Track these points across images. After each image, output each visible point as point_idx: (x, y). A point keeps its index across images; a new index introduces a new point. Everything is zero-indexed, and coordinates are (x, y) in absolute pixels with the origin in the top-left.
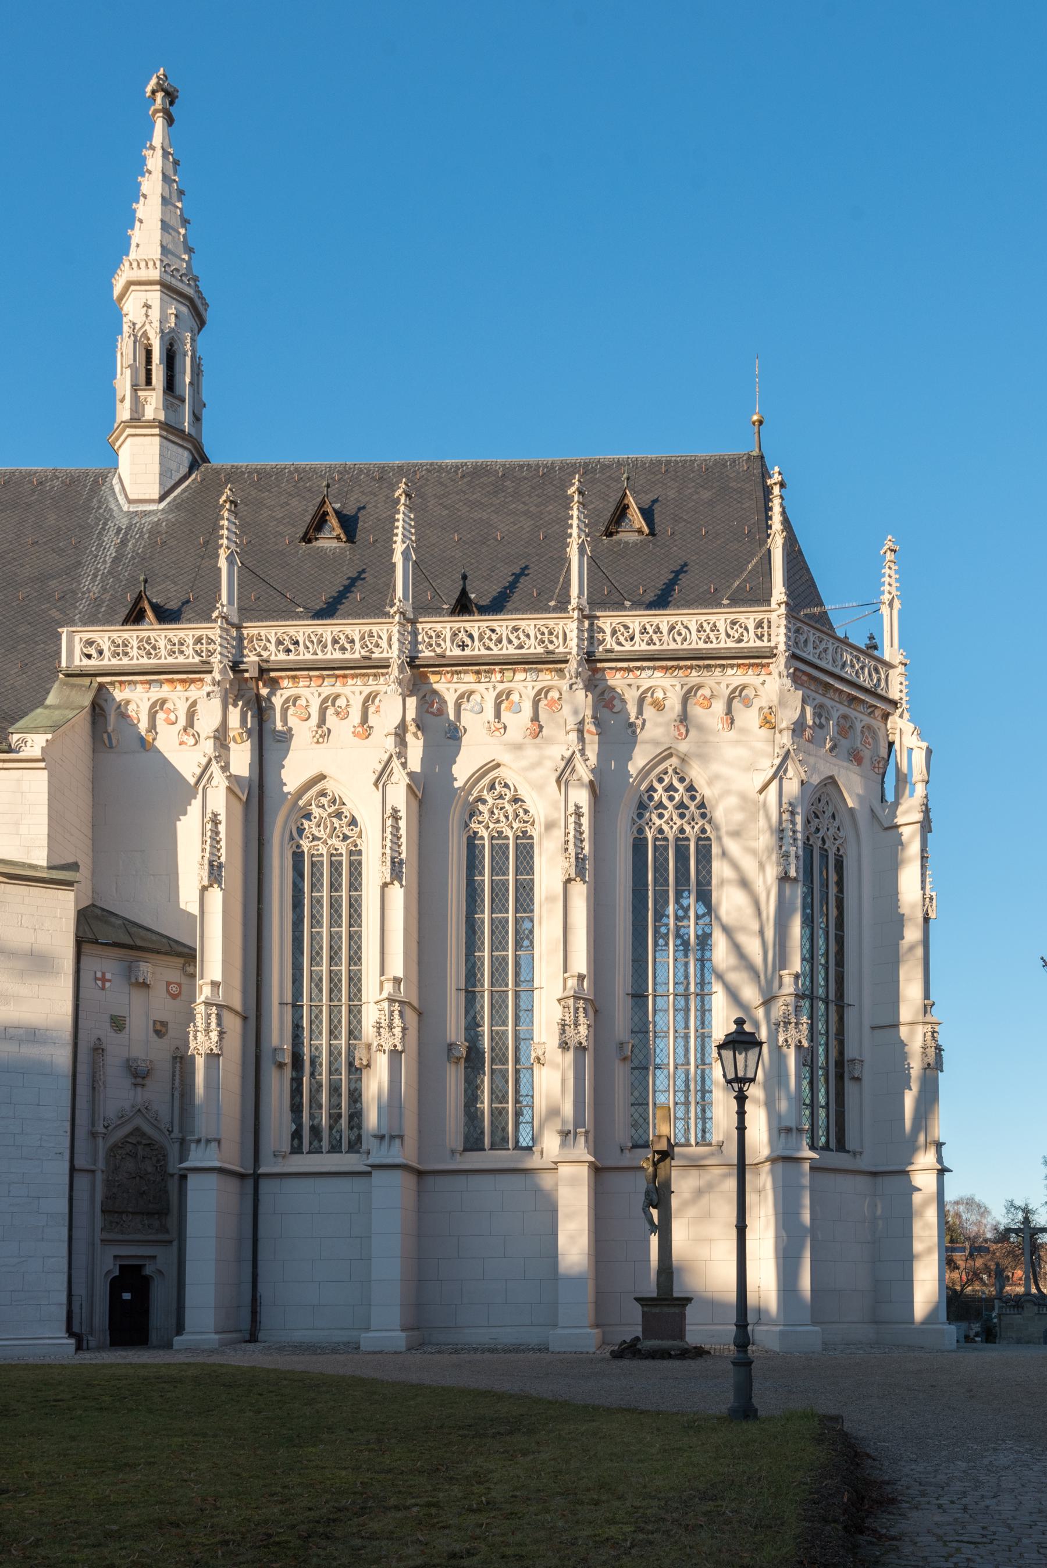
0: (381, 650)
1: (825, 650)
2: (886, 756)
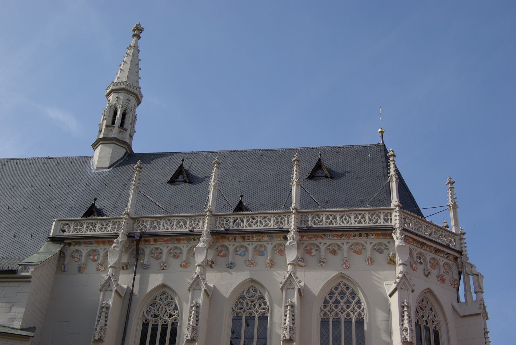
0: (199, 227)
1: (421, 227)
2: (458, 279)
